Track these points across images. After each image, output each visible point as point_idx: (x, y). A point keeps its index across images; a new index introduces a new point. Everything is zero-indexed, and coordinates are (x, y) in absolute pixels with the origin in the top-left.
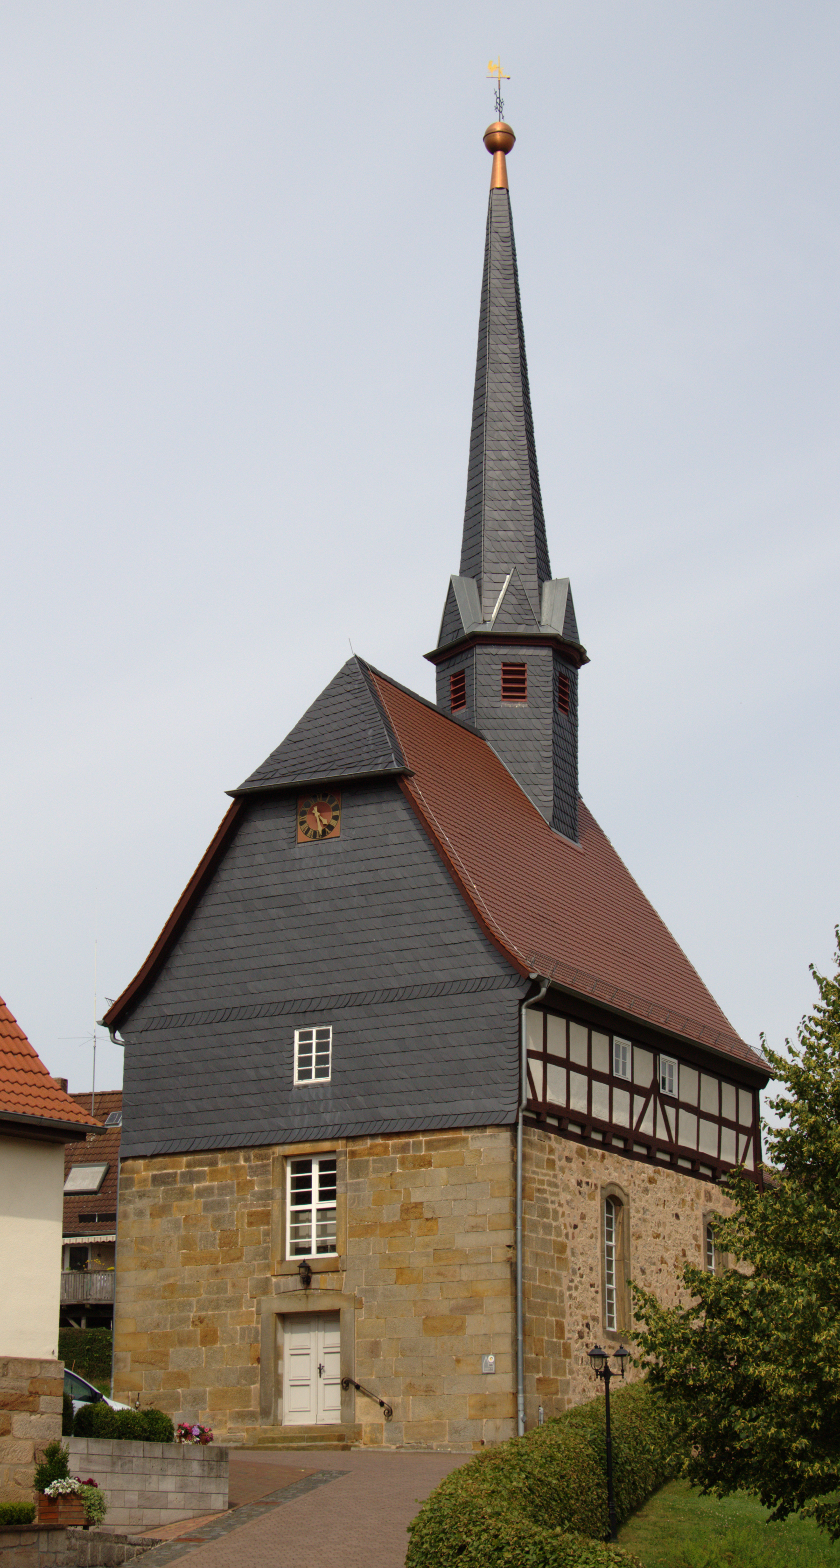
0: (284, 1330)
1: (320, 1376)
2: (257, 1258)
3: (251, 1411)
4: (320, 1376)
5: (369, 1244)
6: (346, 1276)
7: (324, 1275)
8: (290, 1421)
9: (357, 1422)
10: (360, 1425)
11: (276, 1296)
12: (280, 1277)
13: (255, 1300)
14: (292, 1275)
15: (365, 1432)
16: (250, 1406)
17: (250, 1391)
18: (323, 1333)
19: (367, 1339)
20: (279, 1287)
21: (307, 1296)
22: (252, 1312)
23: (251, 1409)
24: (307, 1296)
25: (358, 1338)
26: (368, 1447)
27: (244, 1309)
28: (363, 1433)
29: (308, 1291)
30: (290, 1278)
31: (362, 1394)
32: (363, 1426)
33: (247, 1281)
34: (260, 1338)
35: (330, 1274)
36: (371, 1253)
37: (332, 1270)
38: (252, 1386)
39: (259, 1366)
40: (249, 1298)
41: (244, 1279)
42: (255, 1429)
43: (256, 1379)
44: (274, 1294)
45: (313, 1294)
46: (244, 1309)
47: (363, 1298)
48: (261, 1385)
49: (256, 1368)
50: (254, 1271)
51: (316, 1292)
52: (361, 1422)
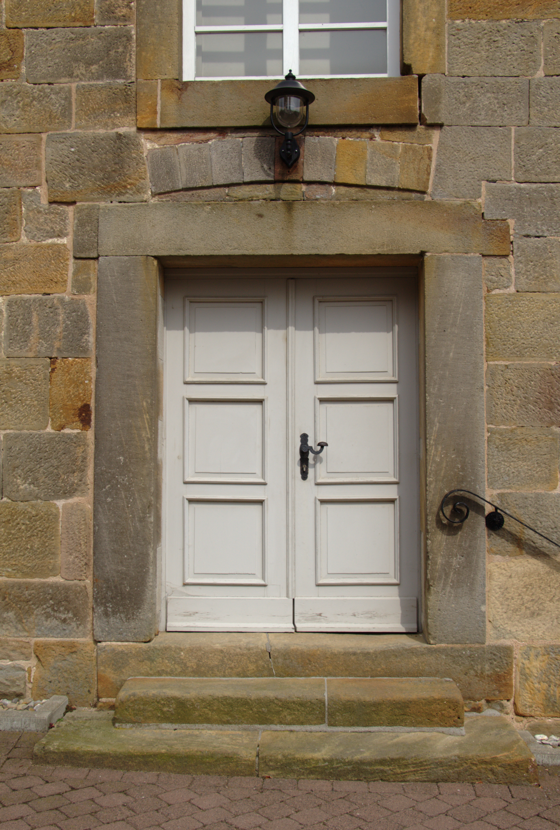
0: (168, 325)
1: (304, 475)
2: (80, 69)
3: (55, 587)
4: (304, 475)
5: (533, 40)
6: (441, 143)
7: (351, 138)
8: (189, 615)
9: (491, 640)
10: (507, 651)
11: (153, 201)
12: (174, 136)
13: (70, 210)
14: (222, 131)
15: (525, 676)
16: (53, 571)
17: (52, 517)
18: (309, 334)
19: (534, 362)
20: (171, 172)
21: (289, 205)
22: (58, 251)
23: (57, 579)
24: (289, 205)
25: (490, 355)
26: (535, 730)
27: (24, 239)
28: (516, 678)
29: (287, 187)
30: (213, 140)
31: (511, 547)
32: (517, 654)
33: (36, 146)
34: (91, 339)
35: (377, 134)
36: (540, 74)
37: (391, 120)
38: (60, 503)
39: (90, 434)
40: (44, 202)
41: (24, 139)
42: (72, 649)
43: (74, 479)
44: (147, 195)
45: (307, 200)
46: (24, 239)
47: (511, 222)
48: (97, 502)
49: (79, 441)
50: (66, 112)
51: (318, 192)
52: (507, 642)
